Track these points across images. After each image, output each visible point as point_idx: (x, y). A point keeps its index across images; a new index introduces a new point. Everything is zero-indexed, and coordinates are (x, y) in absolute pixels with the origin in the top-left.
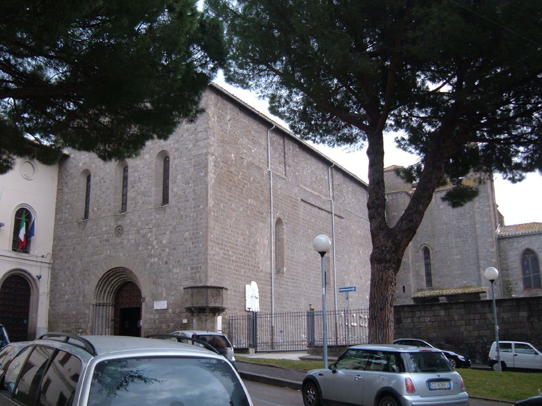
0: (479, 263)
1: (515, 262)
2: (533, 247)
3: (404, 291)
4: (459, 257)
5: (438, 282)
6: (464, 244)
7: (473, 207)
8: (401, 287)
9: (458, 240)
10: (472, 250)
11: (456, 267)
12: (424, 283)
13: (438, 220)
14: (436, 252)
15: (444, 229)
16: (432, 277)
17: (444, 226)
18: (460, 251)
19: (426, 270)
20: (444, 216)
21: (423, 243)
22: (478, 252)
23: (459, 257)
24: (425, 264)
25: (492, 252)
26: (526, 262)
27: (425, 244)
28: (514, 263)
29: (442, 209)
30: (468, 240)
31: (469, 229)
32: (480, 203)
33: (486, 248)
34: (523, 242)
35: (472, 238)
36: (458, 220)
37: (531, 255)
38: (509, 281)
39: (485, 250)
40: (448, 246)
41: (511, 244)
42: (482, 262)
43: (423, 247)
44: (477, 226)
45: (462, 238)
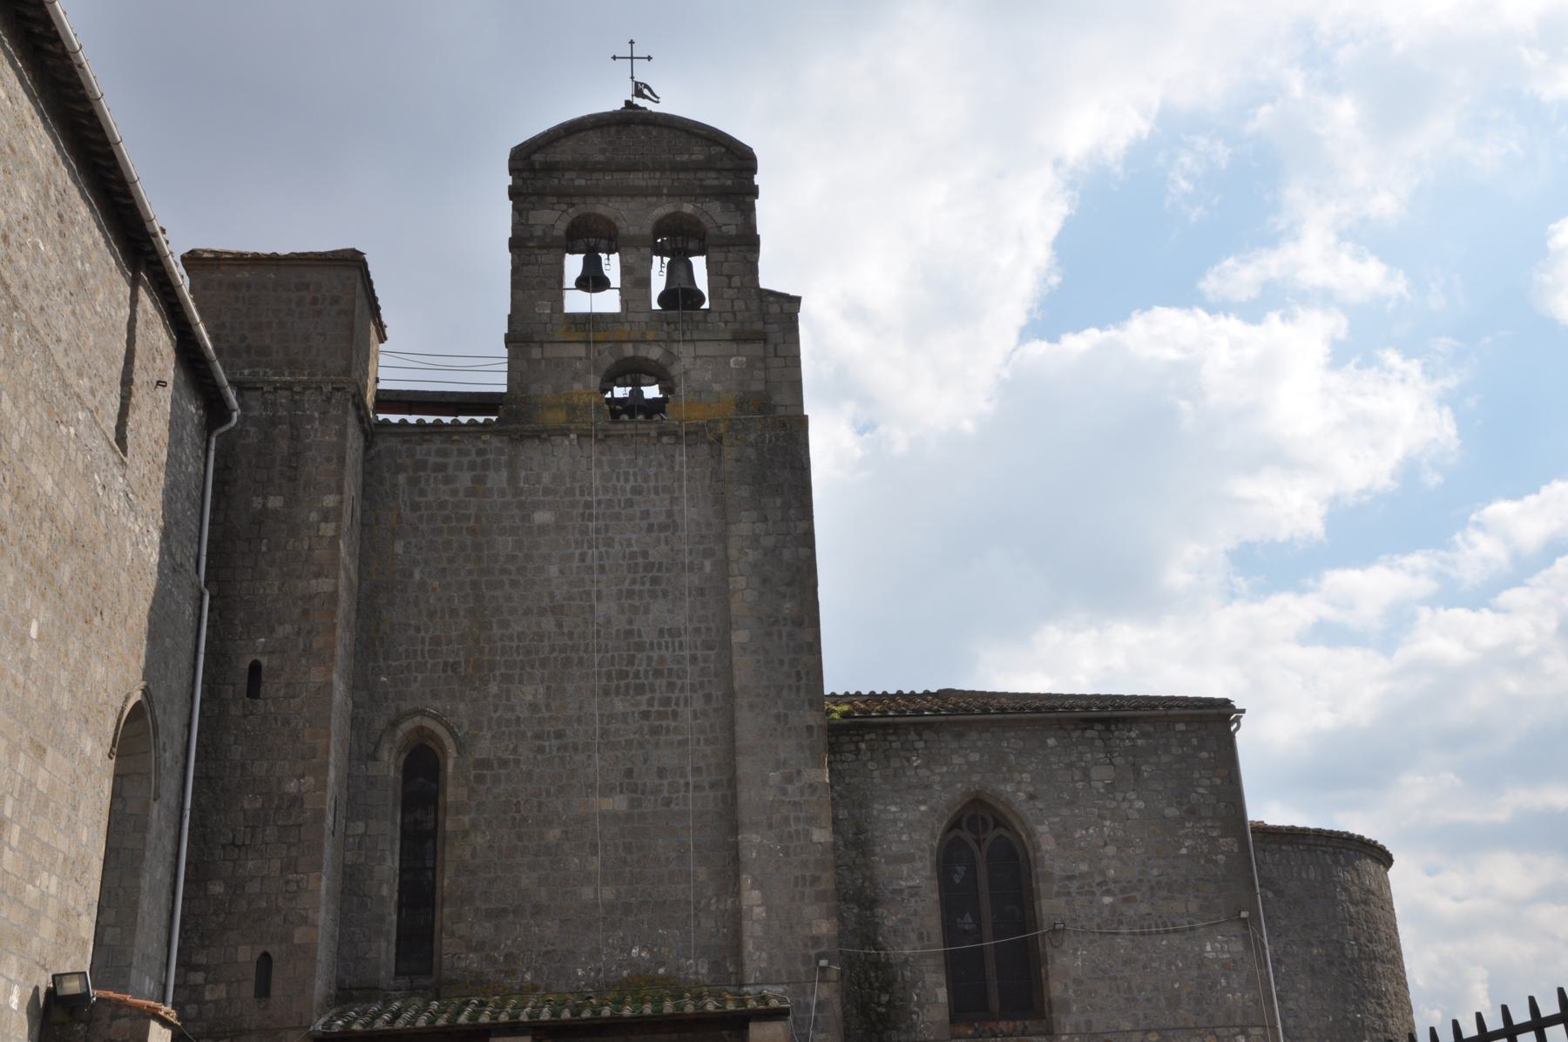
0: (735, 846)
1: (909, 859)
2: (1009, 788)
3: (263, 989)
4: (618, 803)
5: (479, 947)
6: (654, 731)
7: (723, 538)
8: (247, 955)
9: (619, 705)
10: (697, 770)
11: (596, 863)
12: (384, 951)
13: (514, 584)
14: (484, 764)
15: (540, 636)
16: (445, 912)
17: (548, 624)
18: (629, 773)
19: (403, 871)
20: (553, 570)
21: (406, 706)
22: (732, 782)
23: (618, 803)
24: (405, 835)
25: (813, 787)
26: (961, 869)
27: (423, 713)
28: (905, 869)
29: (543, 529)
30: (675, 714)
31: (687, 653)
32: (765, 519)
33: (778, 765)
34: (957, 760)
35: (698, 704)
36: (630, 594)
37: (991, 835)
38: (876, 965)
39: (775, 777)
40: (560, 735)
41: (895, 763)
42: (756, 839)
43: (407, 726)
44: (739, 637)
45: (645, 698)
